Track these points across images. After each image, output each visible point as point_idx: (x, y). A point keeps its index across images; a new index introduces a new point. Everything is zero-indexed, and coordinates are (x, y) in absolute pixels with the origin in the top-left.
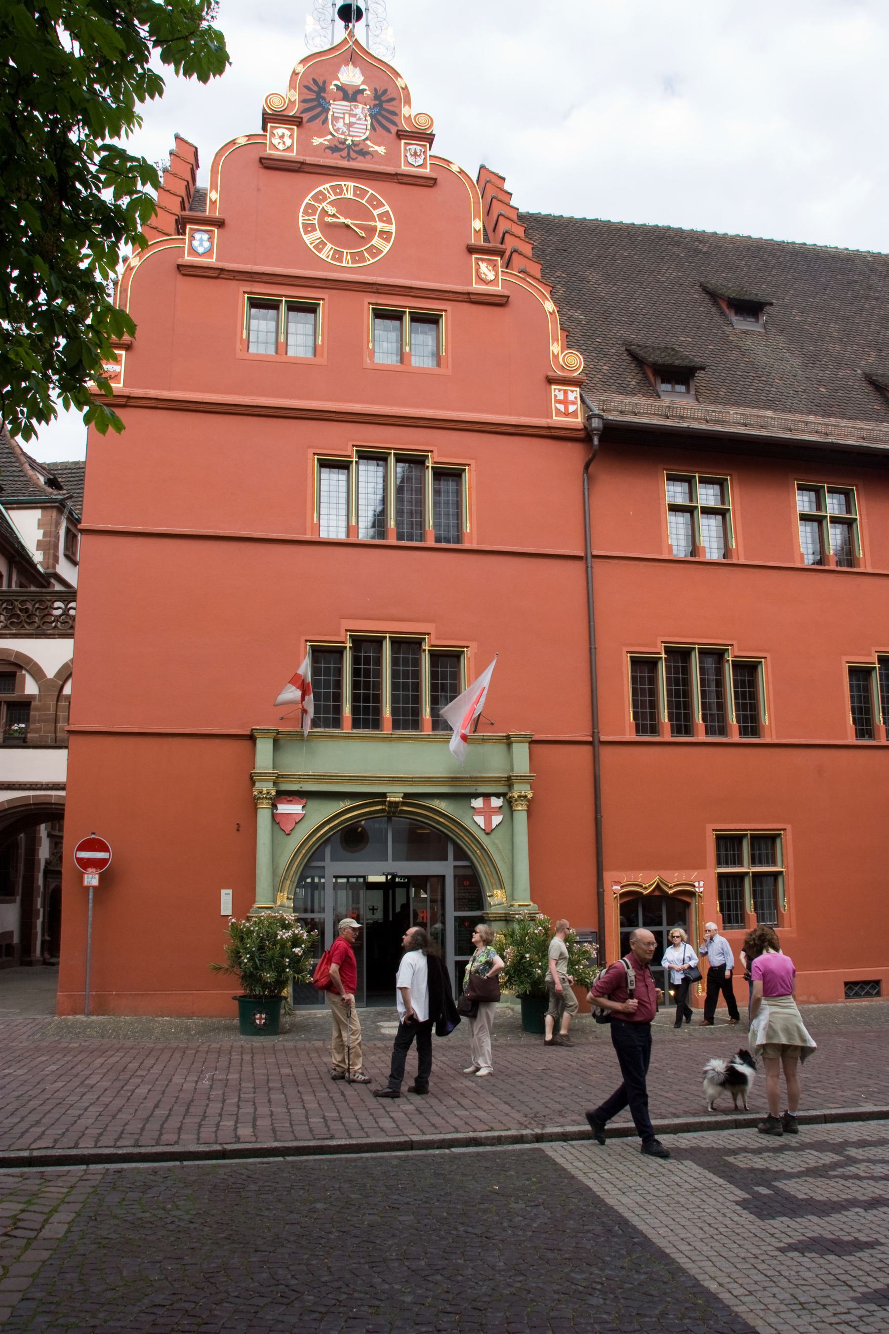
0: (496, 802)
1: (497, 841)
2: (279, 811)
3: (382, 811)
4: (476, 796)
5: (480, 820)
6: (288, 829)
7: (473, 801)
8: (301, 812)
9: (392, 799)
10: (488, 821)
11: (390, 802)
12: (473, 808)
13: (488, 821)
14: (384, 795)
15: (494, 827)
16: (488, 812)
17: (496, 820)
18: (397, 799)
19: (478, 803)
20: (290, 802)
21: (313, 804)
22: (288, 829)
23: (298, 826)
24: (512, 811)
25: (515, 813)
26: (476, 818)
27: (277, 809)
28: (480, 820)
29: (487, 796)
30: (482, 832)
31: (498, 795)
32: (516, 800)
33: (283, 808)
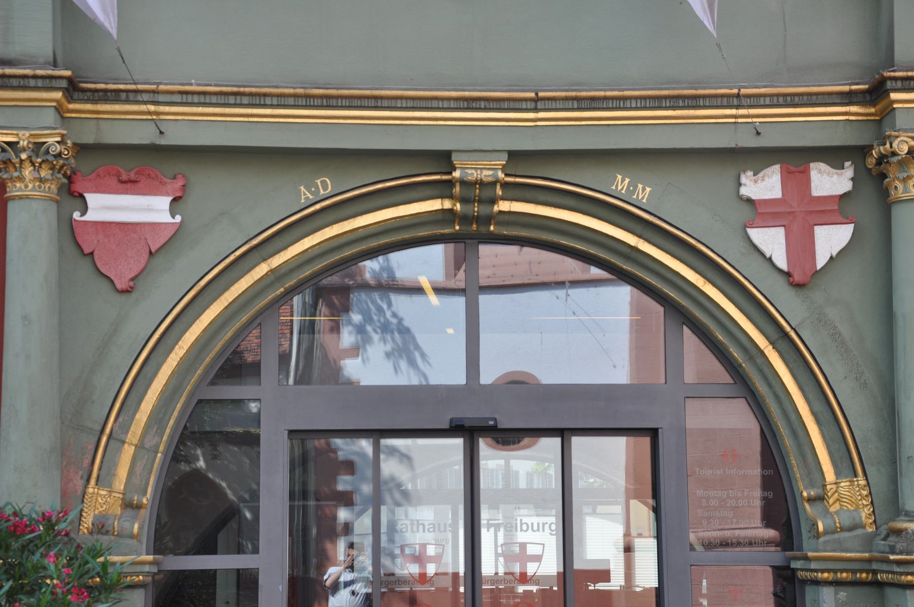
0: (829, 181)
1: (832, 313)
2: (90, 216)
3: (447, 216)
4: (757, 157)
5: (772, 241)
6: (122, 275)
7: (746, 178)
8: (165, 217)
9: (472, 175)
10: (802, 245)
11: (463, 183)
12: (749, 201)
13: (802, 245)
14: (444, 159)
15: (821, 262)
16: (799, 214)
17: (831, 240)
18: (486, 175)
19: (766, 185)
20: (128, 185)
21: (212, 186)
22: (122, 275)
23: (158, 260)
24: (886, 204)
25: (896, 211)
26: (758, 235)
27: (84, 211)
28: (772, 241)
29: (795, 159)
30: (781, 281)
31: (833, 155)
32: (903, 164)
33: (104, 206)
